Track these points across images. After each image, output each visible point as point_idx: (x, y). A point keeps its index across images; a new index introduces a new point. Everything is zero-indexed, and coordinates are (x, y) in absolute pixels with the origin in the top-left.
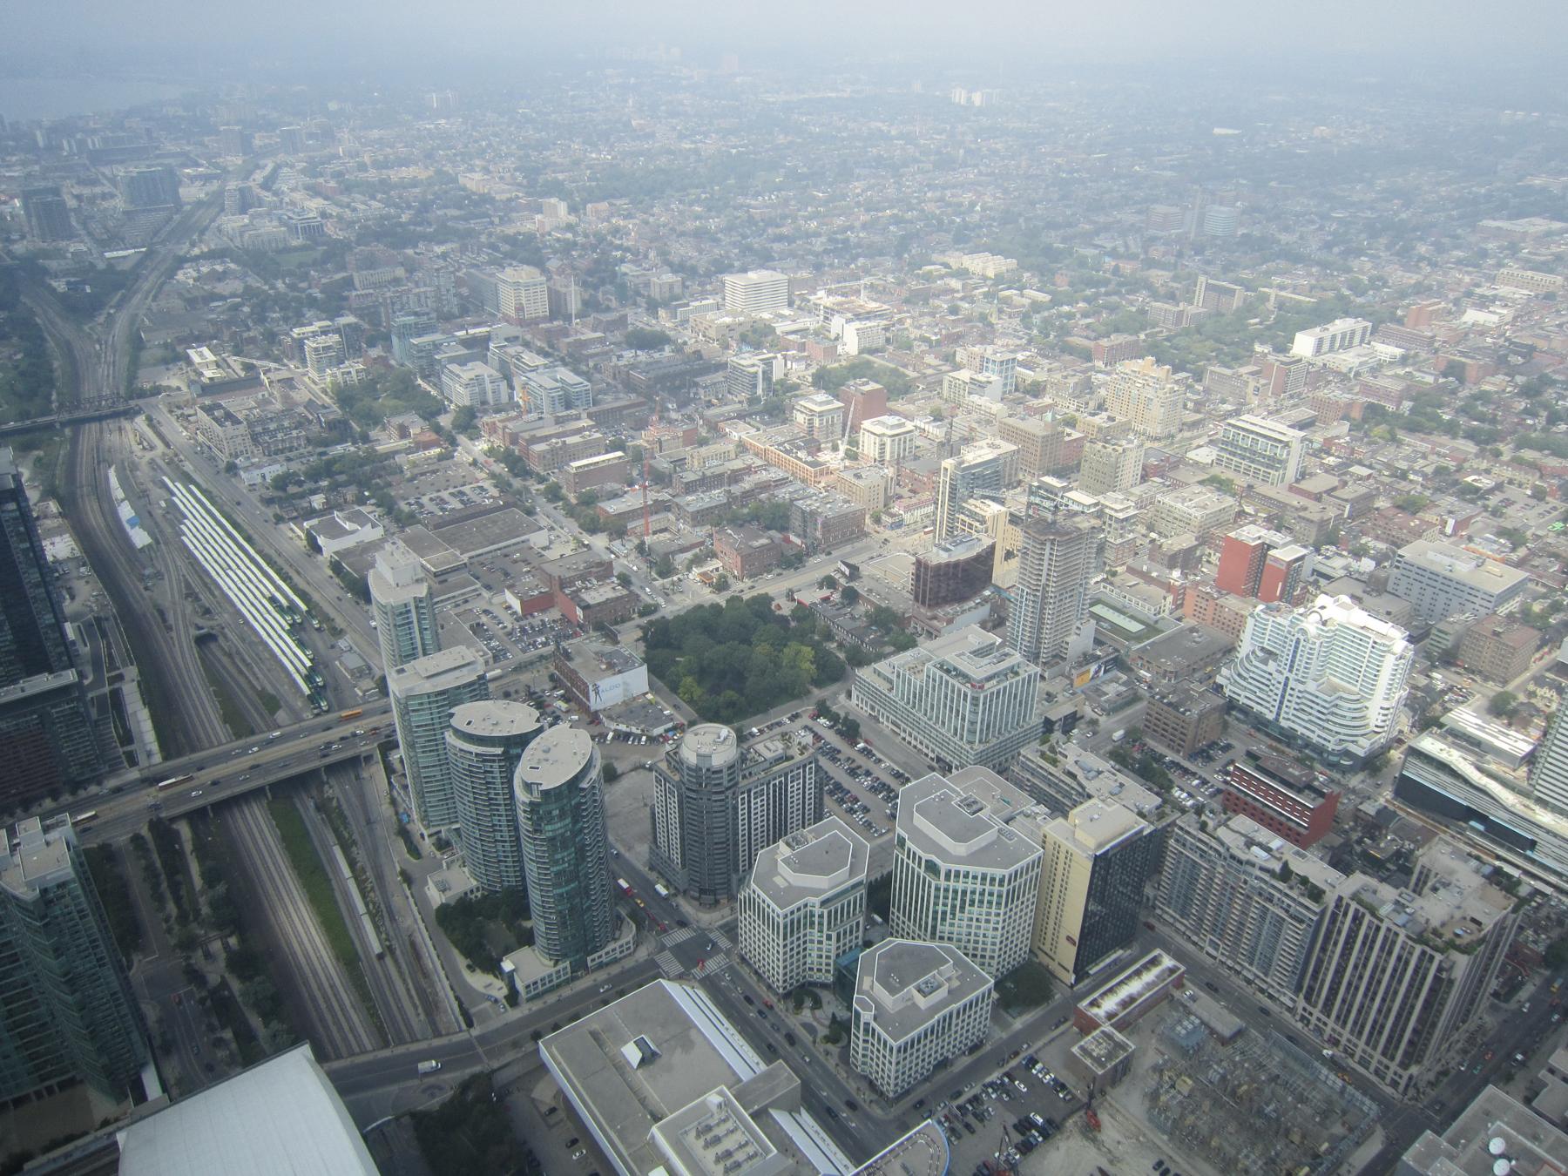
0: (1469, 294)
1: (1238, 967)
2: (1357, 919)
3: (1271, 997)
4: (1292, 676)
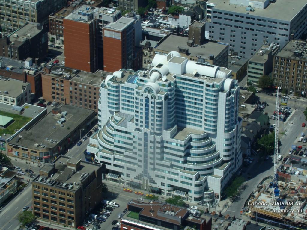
4: (148, 131)
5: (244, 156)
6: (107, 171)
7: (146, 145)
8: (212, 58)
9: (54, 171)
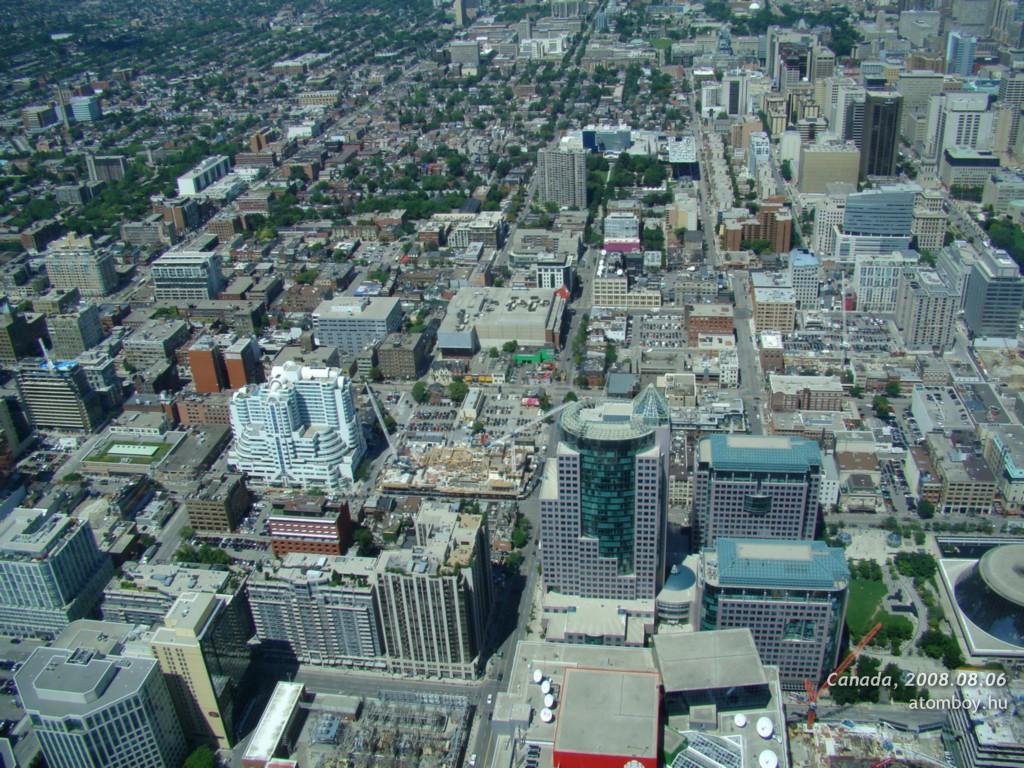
0: (286, 117)
1: (338, 661)
2: (396, 584)
3: (370, 668)
4: (279, 435)
5: (368, 441)
6: (250, 478)
7: (279, 448)
8: (324, 361)
9: (202, 487)
